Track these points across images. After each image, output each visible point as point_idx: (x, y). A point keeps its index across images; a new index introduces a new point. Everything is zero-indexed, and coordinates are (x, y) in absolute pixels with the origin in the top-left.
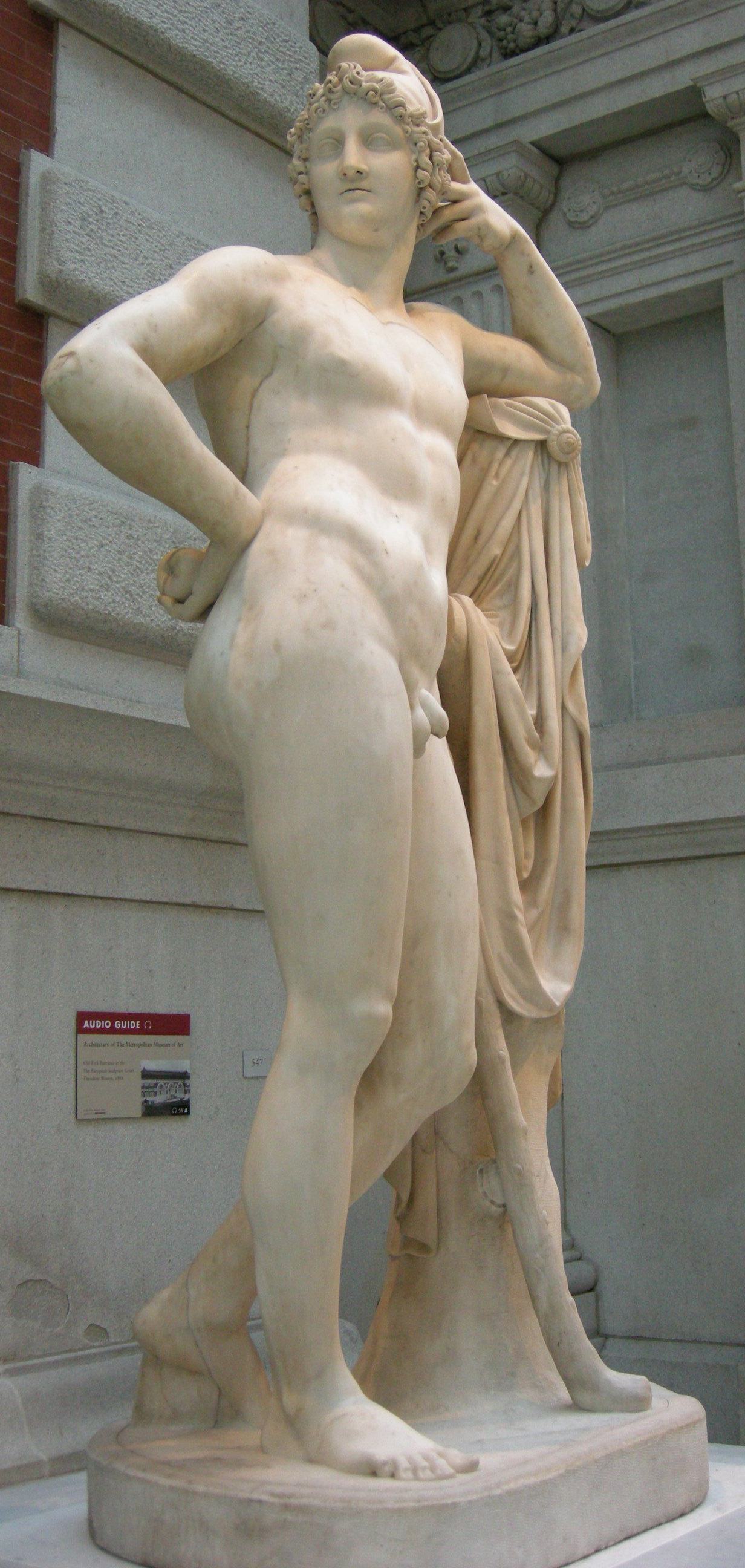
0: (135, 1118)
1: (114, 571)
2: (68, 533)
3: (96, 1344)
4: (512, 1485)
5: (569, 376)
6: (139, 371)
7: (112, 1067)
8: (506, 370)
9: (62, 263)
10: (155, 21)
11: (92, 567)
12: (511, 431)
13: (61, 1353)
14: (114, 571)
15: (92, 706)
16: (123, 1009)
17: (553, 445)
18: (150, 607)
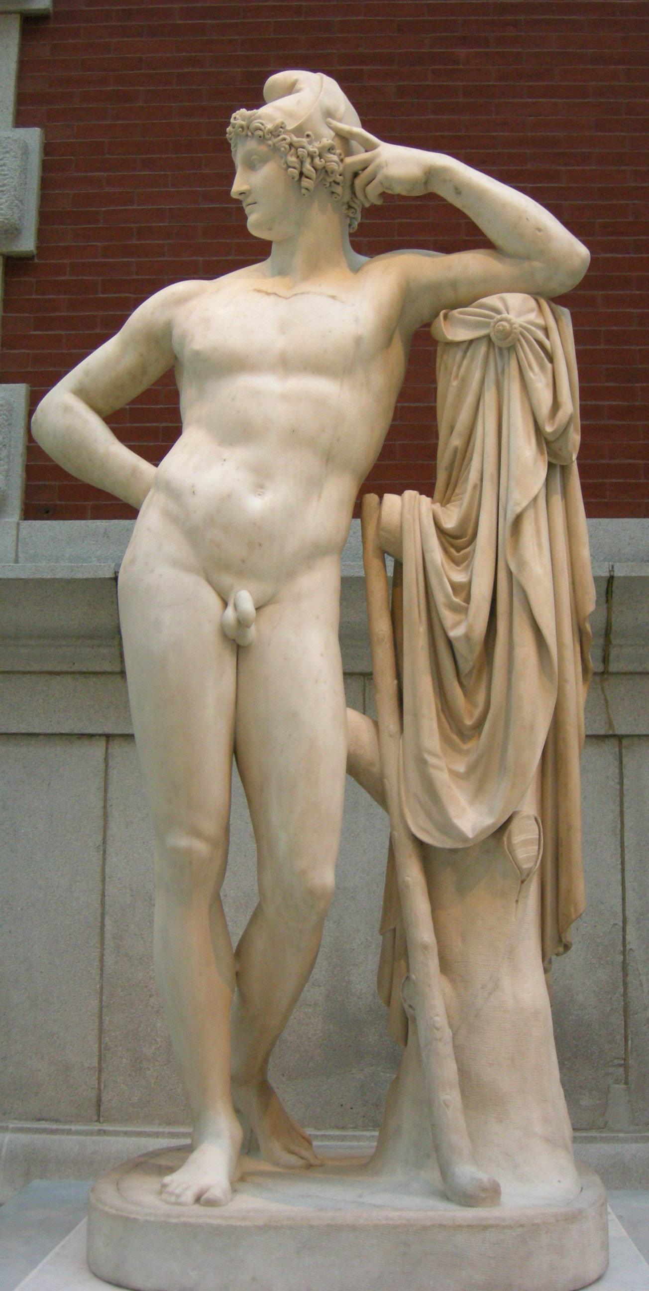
4: (192, 1220)
5: (526, 265)
6: (67, 409)
8: (454, 284)
12: (460, 334)
17: (494, 339)
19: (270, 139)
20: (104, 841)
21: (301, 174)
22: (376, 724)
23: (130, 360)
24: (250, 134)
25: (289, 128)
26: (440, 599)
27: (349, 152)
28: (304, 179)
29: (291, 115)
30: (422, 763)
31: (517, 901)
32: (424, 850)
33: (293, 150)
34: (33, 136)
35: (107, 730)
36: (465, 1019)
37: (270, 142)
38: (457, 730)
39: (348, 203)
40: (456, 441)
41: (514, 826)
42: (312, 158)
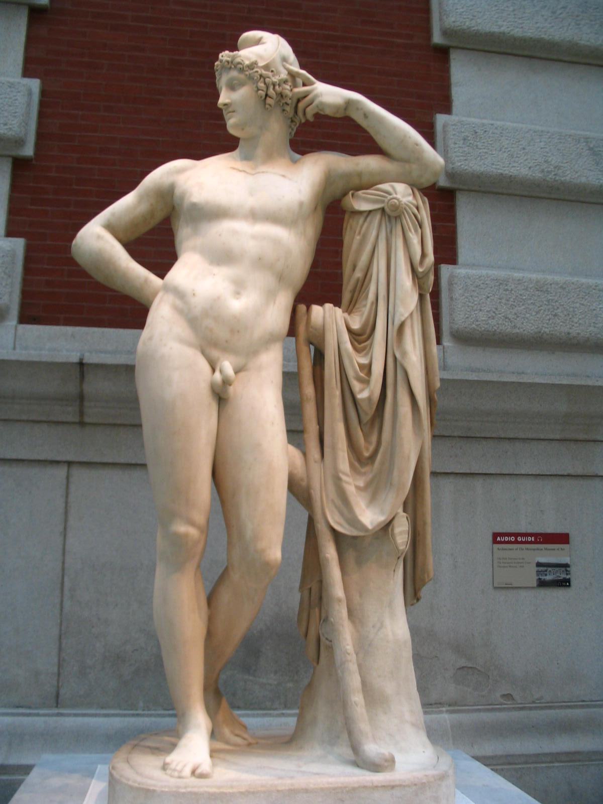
0: (533, 588)
1: (496, 309)
2: (466, 295)
3: (509, 703)
4: (196, 790)
5: (407, 166)
6: (99, 237)
7: (516, 561)
8: (360, 175)
9: (453, 164)
10: (502, 29)
11: (482, 309)
12: (364, 207)
13: (481, 705)
14: (496, 309)
15: (476, 379)
16: (523, 531)
17: (387, 209)
18: (523, 323)
19: (247, 71)
20: (65, 529)
21: (267, 95)
22: (305, 454)
23: (144, 208)
24: (233, 66)
25: (261, 64)
26: (351, 374)
27: (295, 85)
28: (268, 98)
29: (261, 57)
30: (337, 480)
31: (394, 571)
32: (337, 536)
33: (262, 79)
34: (35, 84)
35: (69, 458)
36: (364, 647)
37: (247, 73)
38: (360, 460)
39: (291, 118)
40: (358, 274)
41: (395, 522)
42: (274, 85)
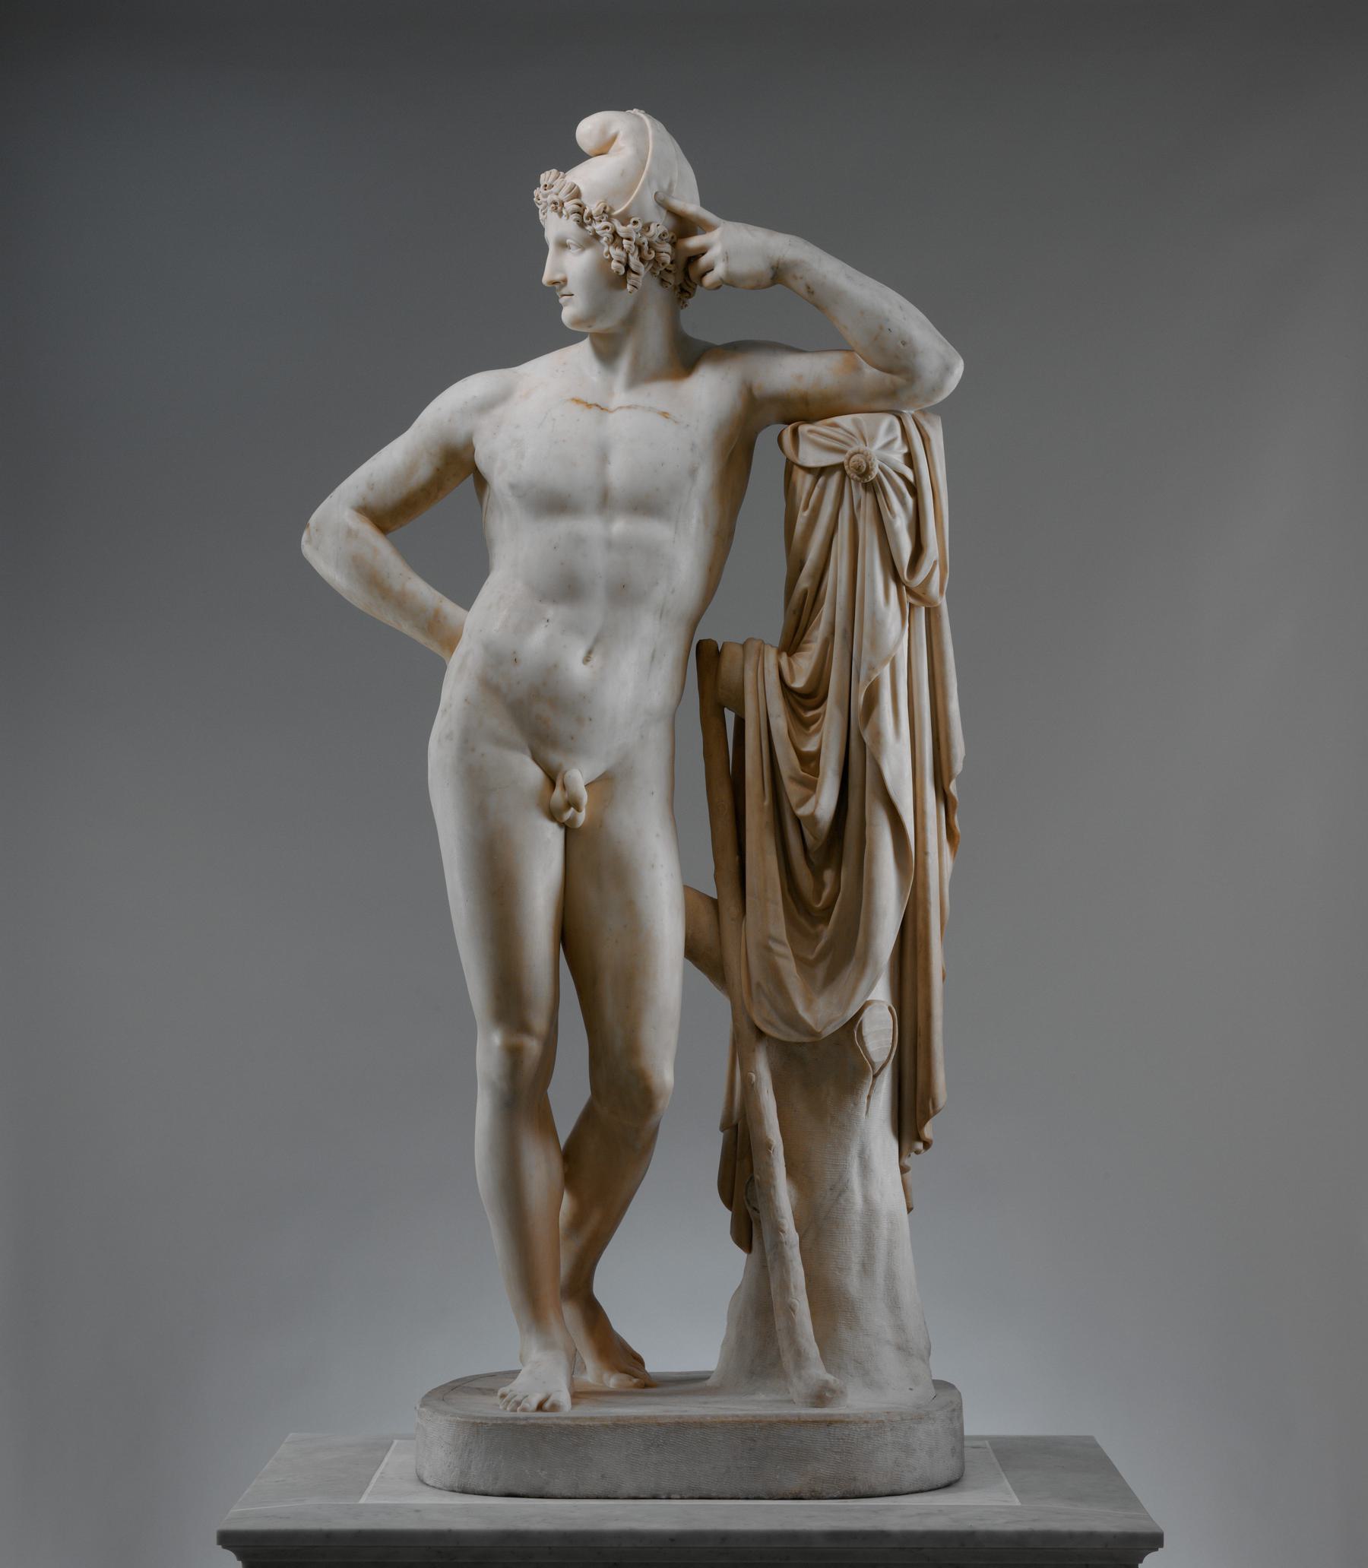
26: (785, 771)
42: (640, 248)
